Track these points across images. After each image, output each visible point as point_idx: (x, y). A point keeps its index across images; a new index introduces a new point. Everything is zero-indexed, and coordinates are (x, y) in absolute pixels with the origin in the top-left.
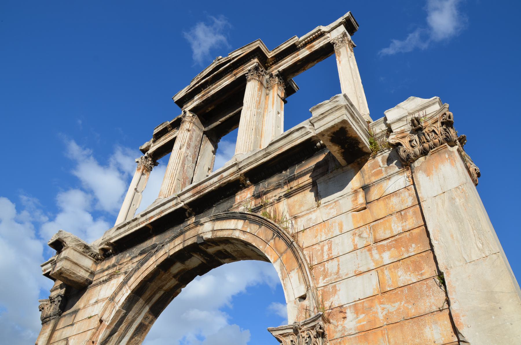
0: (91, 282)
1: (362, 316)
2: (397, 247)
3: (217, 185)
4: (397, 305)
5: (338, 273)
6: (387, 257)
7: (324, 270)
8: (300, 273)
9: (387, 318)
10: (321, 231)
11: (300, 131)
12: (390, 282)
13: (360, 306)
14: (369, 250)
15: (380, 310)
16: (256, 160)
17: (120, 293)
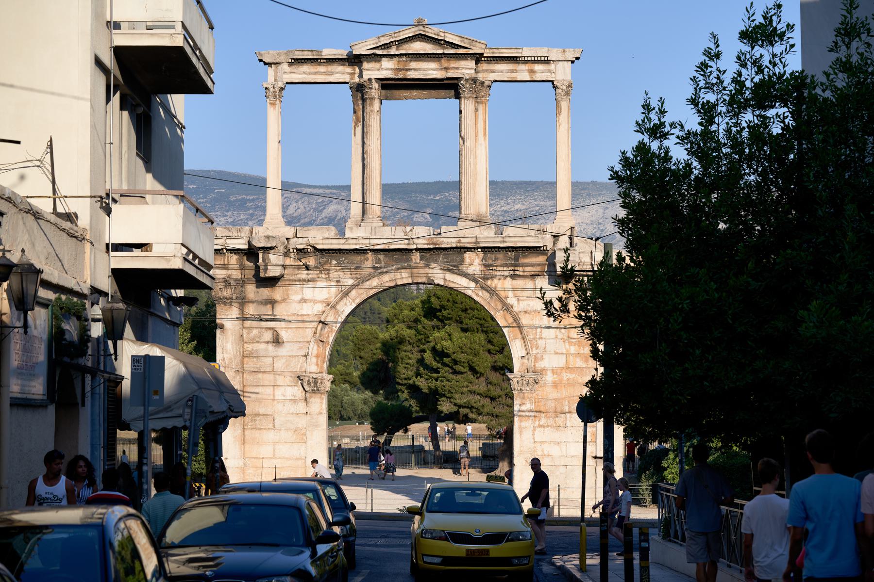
0: (282, 276)
1: (555, 376)
2: (579, 346)
3: (454, 245)
4: (574, 375)
5: (545, 348)
6: (573, 349)
7: (537, 344)
8: (522, 342)
9: (568, 380)
10: (536, 317)
11: (534, 238)
12: (572, 363)
13: (555, 371)
14: (564, 342)
15: (565, 376)
16: (494, 242)
17: (342, 303)
